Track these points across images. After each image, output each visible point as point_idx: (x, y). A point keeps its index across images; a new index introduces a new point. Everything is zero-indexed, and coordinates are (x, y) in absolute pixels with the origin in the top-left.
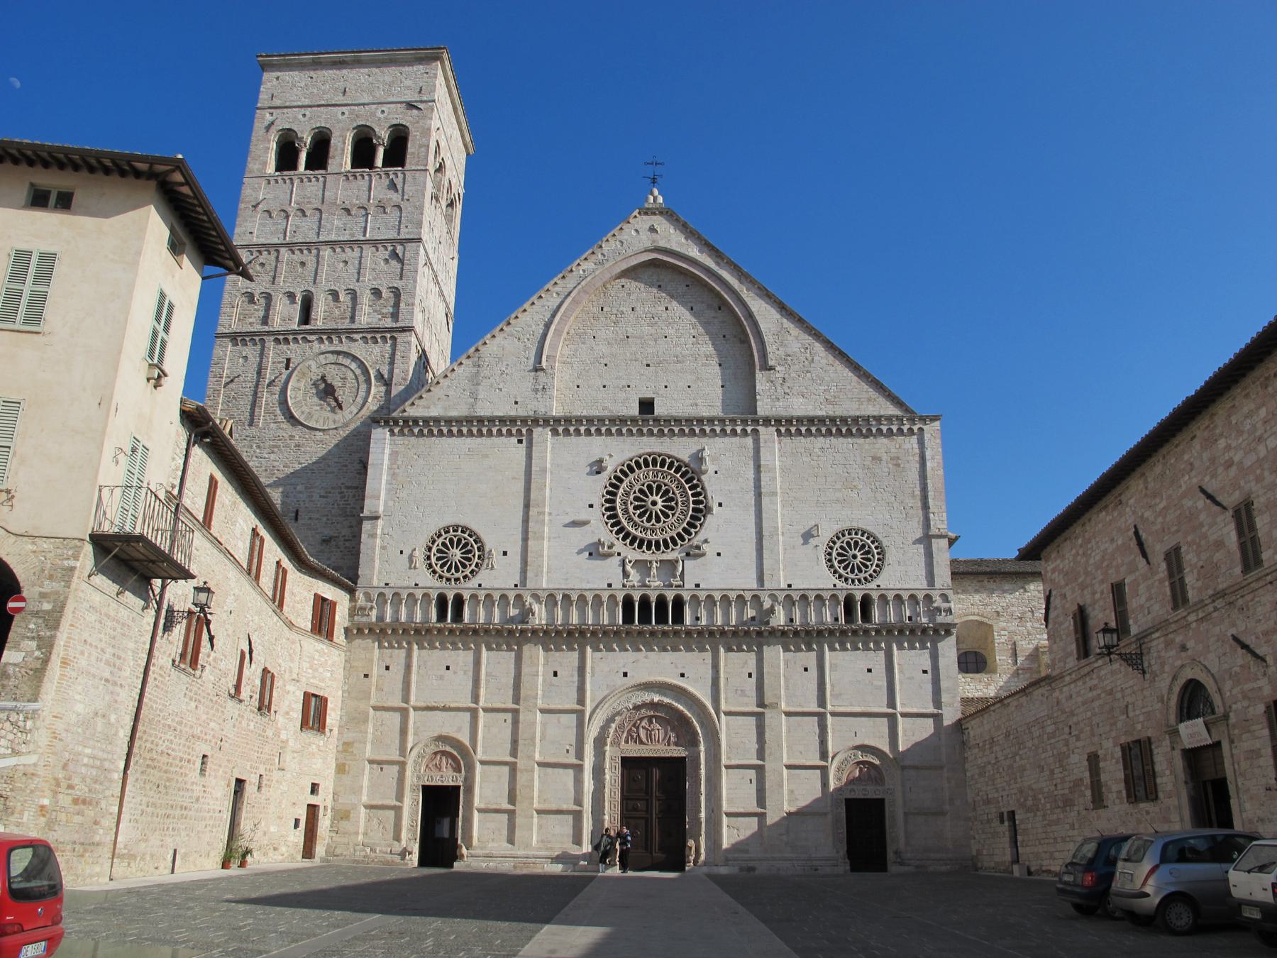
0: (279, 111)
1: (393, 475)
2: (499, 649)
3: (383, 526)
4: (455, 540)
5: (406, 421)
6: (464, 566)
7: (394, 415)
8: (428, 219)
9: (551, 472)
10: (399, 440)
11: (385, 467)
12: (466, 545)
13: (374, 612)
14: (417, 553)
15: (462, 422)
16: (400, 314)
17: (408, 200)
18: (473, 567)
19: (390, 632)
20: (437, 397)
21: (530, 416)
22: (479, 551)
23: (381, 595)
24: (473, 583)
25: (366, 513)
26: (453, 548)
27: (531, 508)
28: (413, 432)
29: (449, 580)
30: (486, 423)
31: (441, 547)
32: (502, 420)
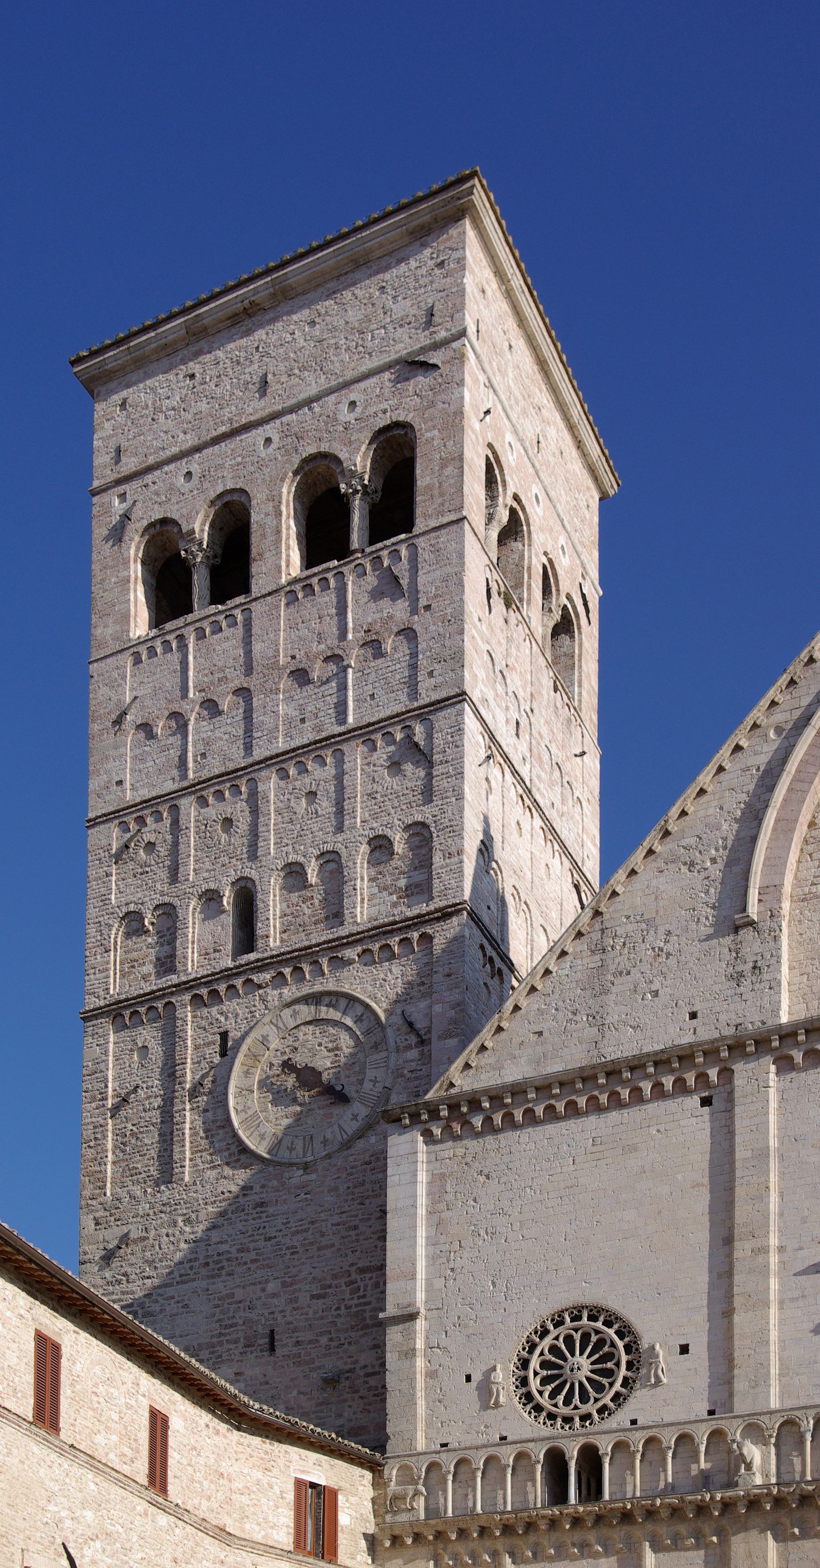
0: (136, 484)
1: (438, 1224)
2: (677, 1545)
3: (427, 1331)
4: (577, 1337)
5: (454, 1107)
6: (599, 1388)
7: (430, 1096)
8: (485, 647)
9: (782, 1157)
10: (448, 1149)
11: (422, 1211)
12: (601, 1343)
13: (420, 1504)
14: (499, 1376)
15: (573, 1083)
16: (436, 882)
17: (428, 608)
18: (617, 1386)
19: (453, 1537)
20: (517, 1041)
21: (723, 1038)
22: (628, 1352)
23: (433, 1467)
24: (621, 1418)
25: (391, 1310)
26: (573, 1354)
27: (737, 1244)
28: (473, 1127)
29: (568, 1420)
30: (627, 1075)
31: (549, 1357)
32: (661, 1061)
